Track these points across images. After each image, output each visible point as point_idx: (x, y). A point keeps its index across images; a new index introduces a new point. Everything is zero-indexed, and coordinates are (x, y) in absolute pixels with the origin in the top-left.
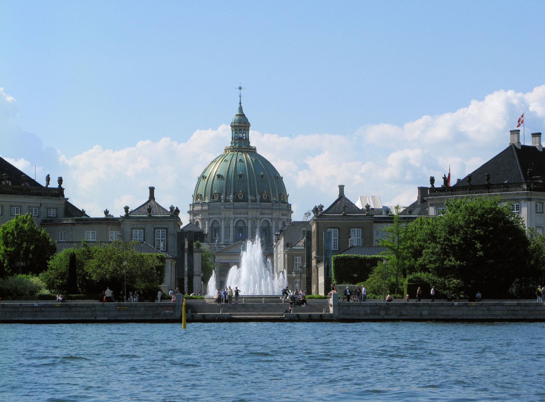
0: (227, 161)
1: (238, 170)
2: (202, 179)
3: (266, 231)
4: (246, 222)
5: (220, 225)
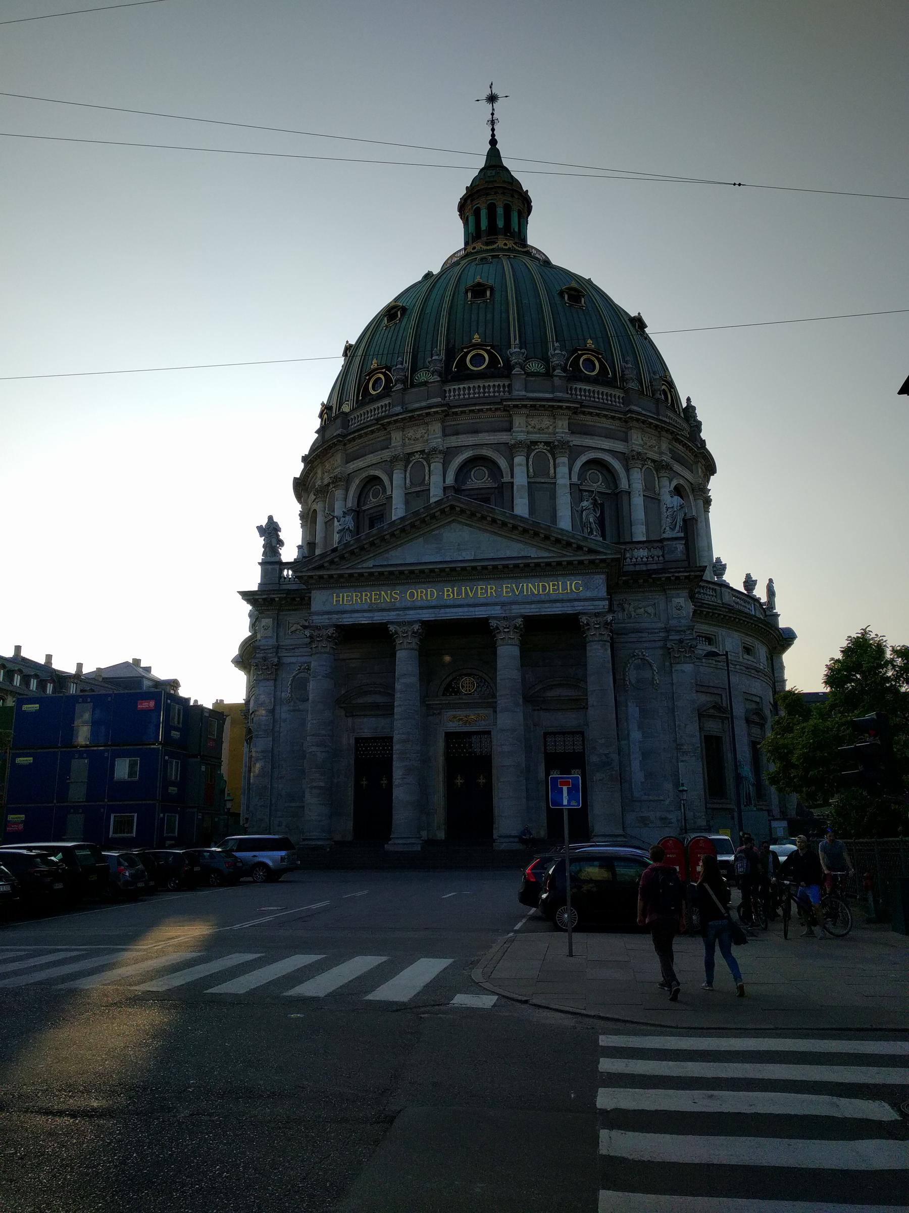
4: (503, 463)
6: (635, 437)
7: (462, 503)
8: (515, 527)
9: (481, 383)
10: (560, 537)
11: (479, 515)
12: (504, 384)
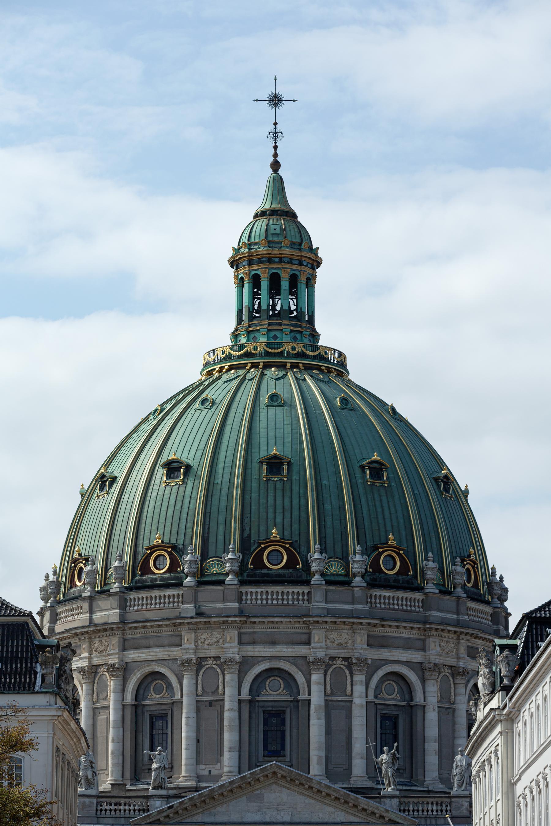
0: (213, 403)
1: (263, 440)
2: (98, 491)
3: (395, 726)
4: (300, 678)
6: (432, 645)
7: (284, 771)
8: (328, 795)
9: (279, 588)
10: (366, 807)
11: (297, 782)
12: (303, 592)
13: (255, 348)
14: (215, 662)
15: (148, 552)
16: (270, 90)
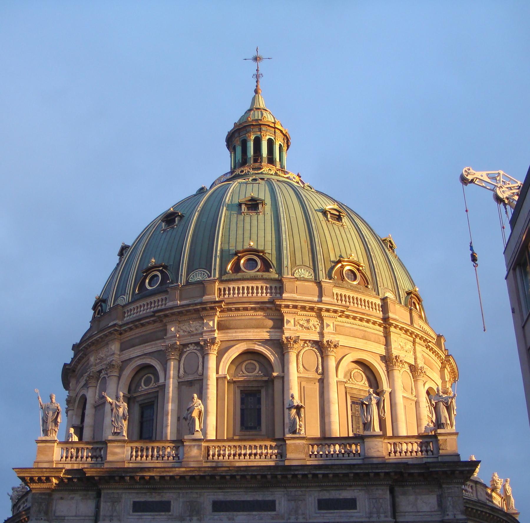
5: (162, 380)
13: (242, 171)
14: (196, 347)
15: (144, 274)
16: (255, 54)
